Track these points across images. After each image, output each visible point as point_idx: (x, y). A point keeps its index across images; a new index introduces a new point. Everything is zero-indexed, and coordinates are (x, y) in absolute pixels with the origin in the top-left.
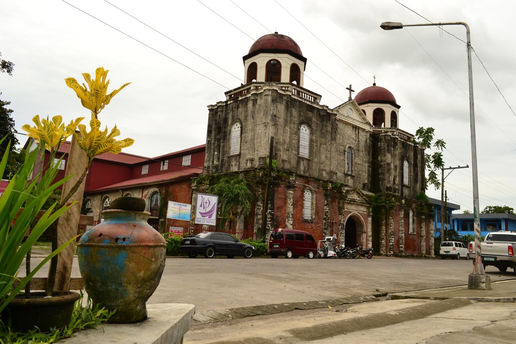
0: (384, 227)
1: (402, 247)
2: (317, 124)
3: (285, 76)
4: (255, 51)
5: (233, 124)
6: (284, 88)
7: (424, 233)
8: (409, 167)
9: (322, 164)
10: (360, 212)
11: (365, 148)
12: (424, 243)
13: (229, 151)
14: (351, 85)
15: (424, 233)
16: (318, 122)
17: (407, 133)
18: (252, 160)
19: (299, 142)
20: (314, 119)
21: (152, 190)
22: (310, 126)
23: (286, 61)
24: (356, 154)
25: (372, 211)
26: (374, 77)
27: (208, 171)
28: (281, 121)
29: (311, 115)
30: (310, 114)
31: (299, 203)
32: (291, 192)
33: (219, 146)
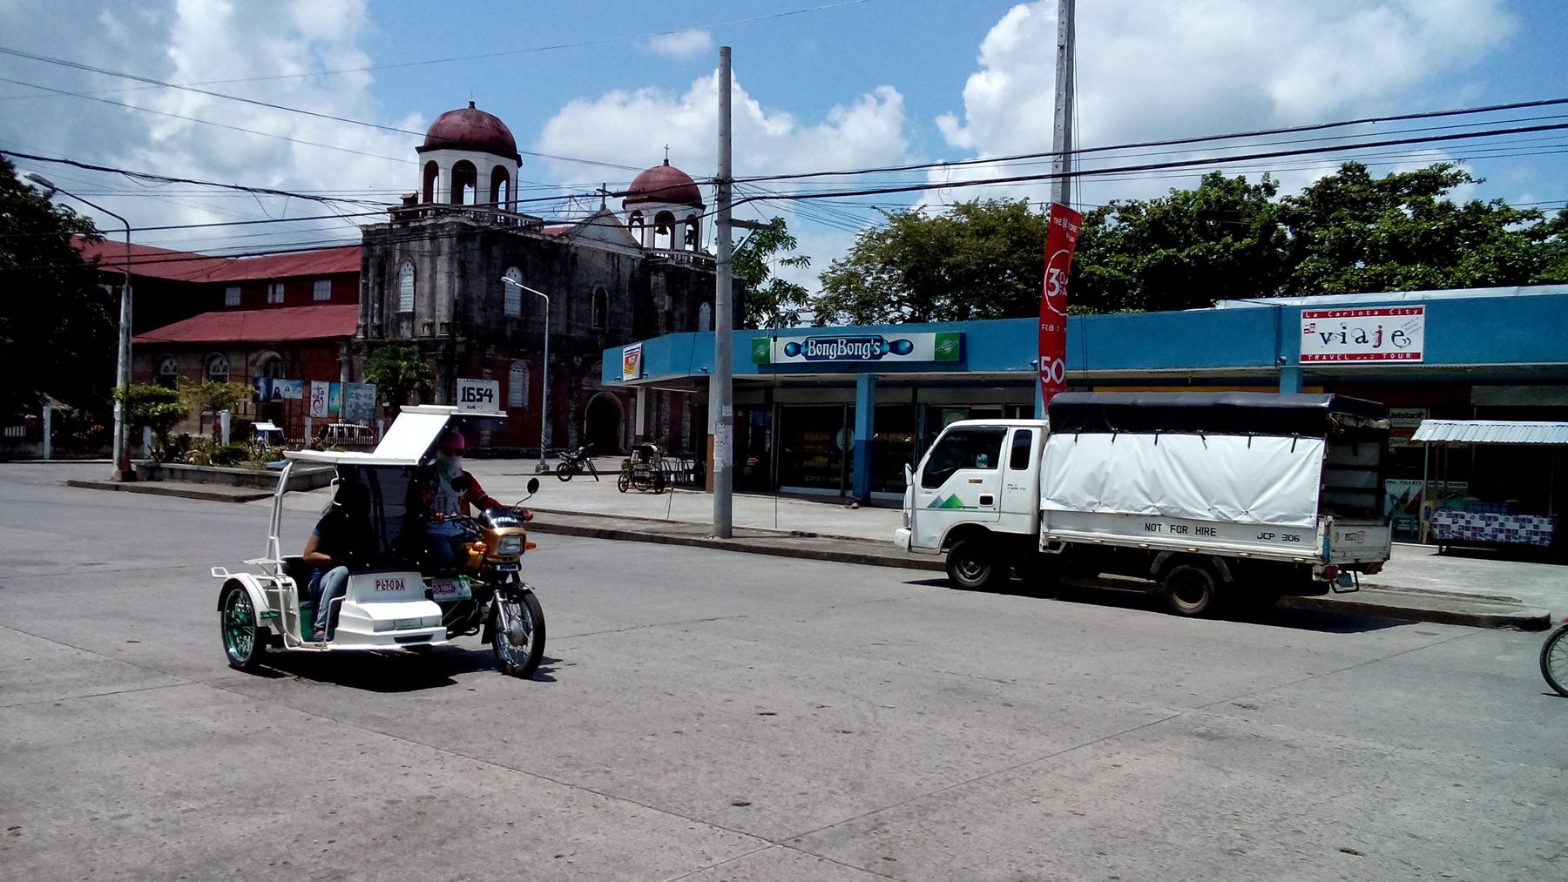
4: (435, 142)
5: (401, 263)
13: (397, 305)
18: (431, 326)
20: (529, 257)
21: (267, 355)
23: (484, 163)
27: (365, 333)
28: (474, 267)
33: (381, 294)
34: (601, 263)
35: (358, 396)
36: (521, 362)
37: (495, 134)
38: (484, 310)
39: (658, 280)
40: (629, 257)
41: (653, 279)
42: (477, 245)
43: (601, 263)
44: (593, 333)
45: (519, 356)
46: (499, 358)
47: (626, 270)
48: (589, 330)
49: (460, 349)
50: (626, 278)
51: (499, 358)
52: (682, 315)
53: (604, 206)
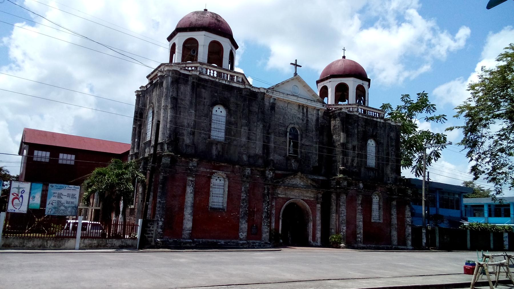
0: (334, 215)
1: (359, 237)
2: (237, 104)
3: (203, 54)
6: (190, 69)
7: (394, 221)
8: (376, 147)
9: (242, 147)
10: (305, 199)
11: (316, 128)
12: (394, 233)
13: (145, 138)
14: (296, 60)
15: (394, 221)
16: (239, 103)
17: (373, 109)
19: (210, 124)
20: (232, 100)
22: (226, 106)
24: (304, 135)
25: (322, 197)
26: (344, 50)
29: (229, 96)
30: (227, 94)
31: (203, 191)
32: (191, 178)
34: (294, 111)
35: (60, 196)
36: (220, 173)
37: (213, 21)
38: (193, 134)
39: (336, 123)
40: (315, 108)
41: (333, 123)
42: (189, 88)
43: (294, 111)
44: (288, 159)
45: (219, 168)
46: (202, 169)
47: (312, 117)
48: (285, 156)
49: (166, 161)
50: (312, 124)
51: (202, 169)
52: (354, 148)
53: (296, 74)
